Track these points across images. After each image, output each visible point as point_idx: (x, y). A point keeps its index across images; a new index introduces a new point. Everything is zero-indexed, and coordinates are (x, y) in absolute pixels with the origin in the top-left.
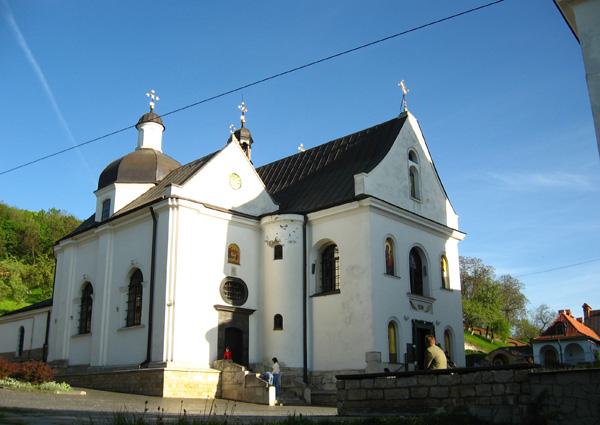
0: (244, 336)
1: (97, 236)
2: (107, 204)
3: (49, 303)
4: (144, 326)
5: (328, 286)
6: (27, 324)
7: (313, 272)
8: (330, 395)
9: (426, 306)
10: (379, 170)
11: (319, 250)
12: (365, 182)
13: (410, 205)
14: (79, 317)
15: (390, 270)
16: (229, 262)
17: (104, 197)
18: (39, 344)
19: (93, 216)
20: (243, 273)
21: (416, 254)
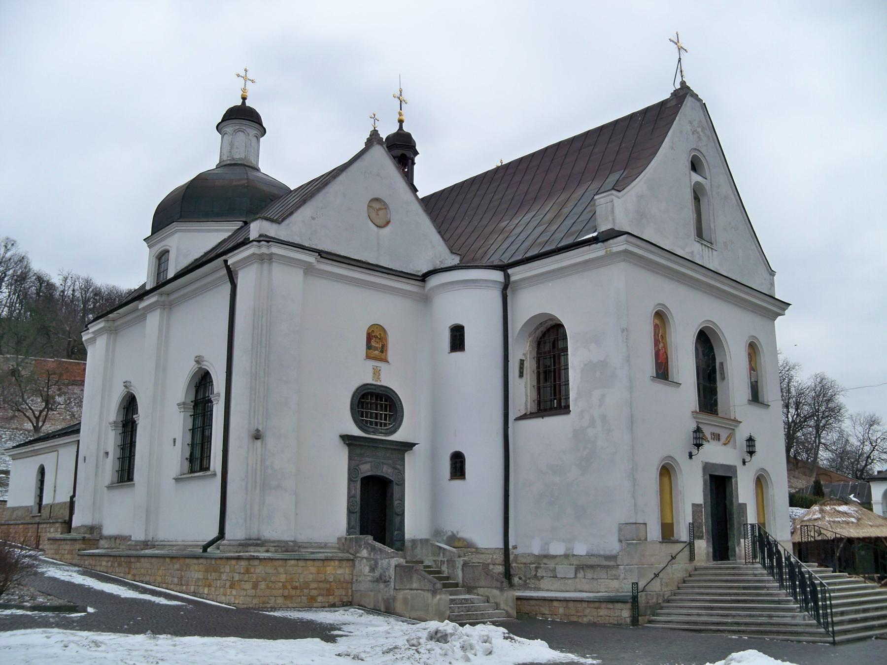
0: (396, 489)
3: (78, 431)
4: (214, 475)
5: (552, 397)
6: (48, 460)
7: (521, 375)
9: (724, 434)
10: (639, 185)
12: (617, 208)
13: (693, 249)
14: (118, 453)
15: (663, 372)
16: (368, 357)
17: (159, 248)
18: (63, 497)
21: (706, 341)
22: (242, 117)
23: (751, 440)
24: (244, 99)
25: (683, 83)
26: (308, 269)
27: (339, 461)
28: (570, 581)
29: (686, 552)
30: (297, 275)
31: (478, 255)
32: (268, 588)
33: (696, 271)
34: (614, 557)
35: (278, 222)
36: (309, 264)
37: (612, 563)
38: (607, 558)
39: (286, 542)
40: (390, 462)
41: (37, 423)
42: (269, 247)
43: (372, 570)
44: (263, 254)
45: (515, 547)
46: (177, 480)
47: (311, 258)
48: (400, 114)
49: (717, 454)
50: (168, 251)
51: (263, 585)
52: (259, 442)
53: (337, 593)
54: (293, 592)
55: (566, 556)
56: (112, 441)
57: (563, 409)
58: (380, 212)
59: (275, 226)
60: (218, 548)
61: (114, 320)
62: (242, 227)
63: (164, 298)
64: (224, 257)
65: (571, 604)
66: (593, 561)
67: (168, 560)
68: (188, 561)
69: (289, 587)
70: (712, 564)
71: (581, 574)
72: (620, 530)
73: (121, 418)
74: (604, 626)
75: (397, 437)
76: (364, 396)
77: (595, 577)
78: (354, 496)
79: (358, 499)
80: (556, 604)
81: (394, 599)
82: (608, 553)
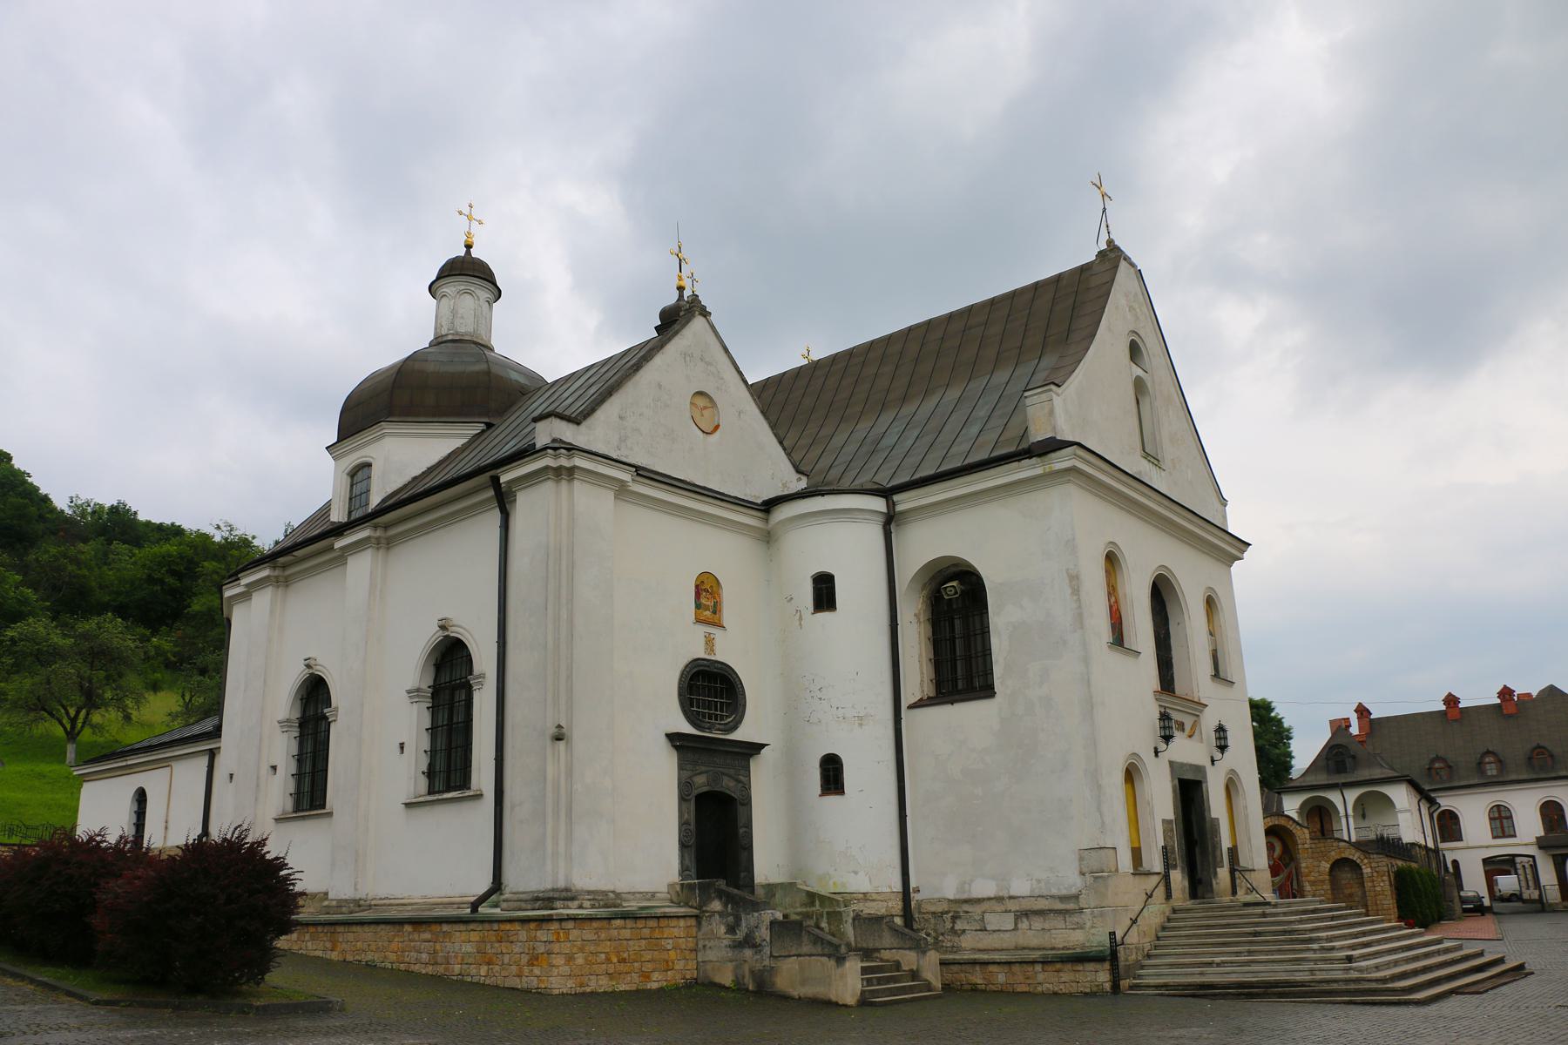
0: (741, 809)
1: (341, 558)
2: (359, 474)
3: (216, 733)
4: (479, 796)
12: (1063, 410)
14: (293, 769)
15: (1118, 639)
16: (698, 621)
19: (326, 509)
20: (732, 649)
21: (1162, 594)
22: (466, 271)
23: (1221, 729)
24: (469, 247)
25: (1110, 242)
26: (621, 490)
27: (665, 769)
28: (1007, 935)
29: (1162, 888)
30: (607, 497)
31: (829, 478)
32: (588, 962)
33: (1149, 498)
34: (1076, 897)
35: (576, 420)
36: (622, 483)
37: (1071, 906)
38: (1063, 899)
39: (605, 893)
40: (732, 772)
41: (73, 727)
42: (570, 457)
43: (731, 930)
44: (560, 467)
45: (917, 891)
46: (408, 805)
47: (625, 476)
48: (680, 279)
49: (1188, 750)
50: (369, 465)
51: (580, 960)
52: (562, 744)
53: (679, 965)
54: (621, 967)
55: (999, 899)
56: (282, 749)
57: (986, 690)
58: (706, 413)
59: (572, 427)
60: (496, 906)
61: (284, 567)
62: (483, 432)
63: (378, 533)
64: (492, 473)
65: (1016, 968)
66: (1042, 904)
67: (408, 928)
68: (445, 928)
69: (615, 960)
70: (1189, 904)
71: (1024, 924)
72: (1081, 859)
73: (297, 714)
74: (1071, 995)
75: (737, 735)
76: (697, 674)
77: (1047, 926)
79: (692, 827)
80: (992, 968)
81: (772, 970)
82: (1064, 892)
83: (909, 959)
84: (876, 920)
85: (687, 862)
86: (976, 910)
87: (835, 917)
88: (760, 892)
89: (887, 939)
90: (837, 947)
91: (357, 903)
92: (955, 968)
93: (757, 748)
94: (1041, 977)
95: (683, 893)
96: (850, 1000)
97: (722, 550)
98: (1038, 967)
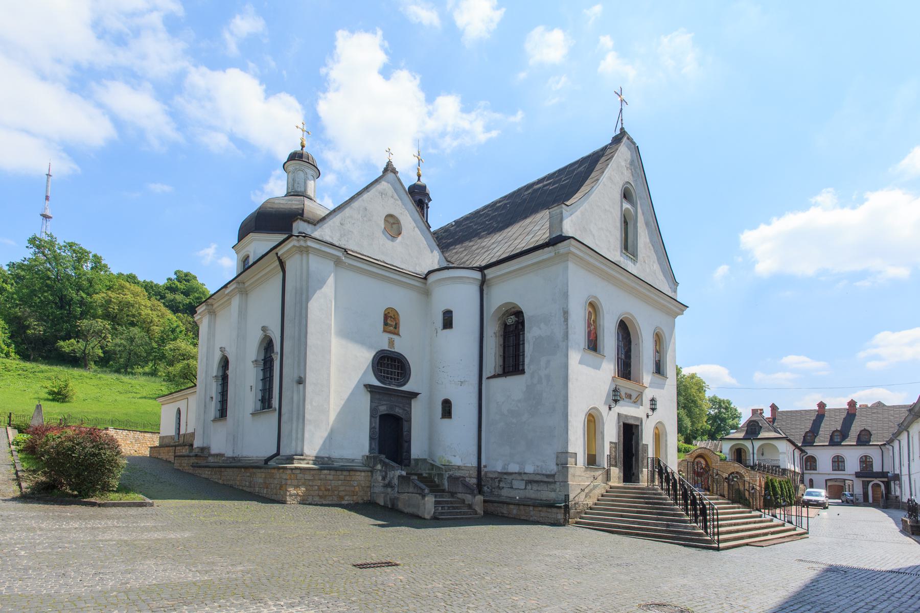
0: (405, 424)
5: (512, 362)
8: (508, 504)
11: (499, 319)
34: (553, 476)
37: (551, 480)
38: (548, 476)
43: (384, 478)
45: (485, 467)
54: (327, 493)
55: (520, 474)
57: (522, 372)
65: (522, 507)
66: (538, 478)
68: (254, 470)
71: (529, 487)
72: (557, 457)
76: (382, 358)
78: (374, 428)
79: (377, 430)
80: (512, 507)
83: (468, 498)
84: (457, 478)
85: (373, 446)
86: (510, 478)
87: (440, 476)
88: (413, 462)
89: (460, 489)
90: (423, 490)
91: (233, 458)
92: (496, 505)
93: (415, 395)
94: (532, 513)
95: (370, 461)
96: (427, 517)
97: (401, 300)
98: (531, 508)
